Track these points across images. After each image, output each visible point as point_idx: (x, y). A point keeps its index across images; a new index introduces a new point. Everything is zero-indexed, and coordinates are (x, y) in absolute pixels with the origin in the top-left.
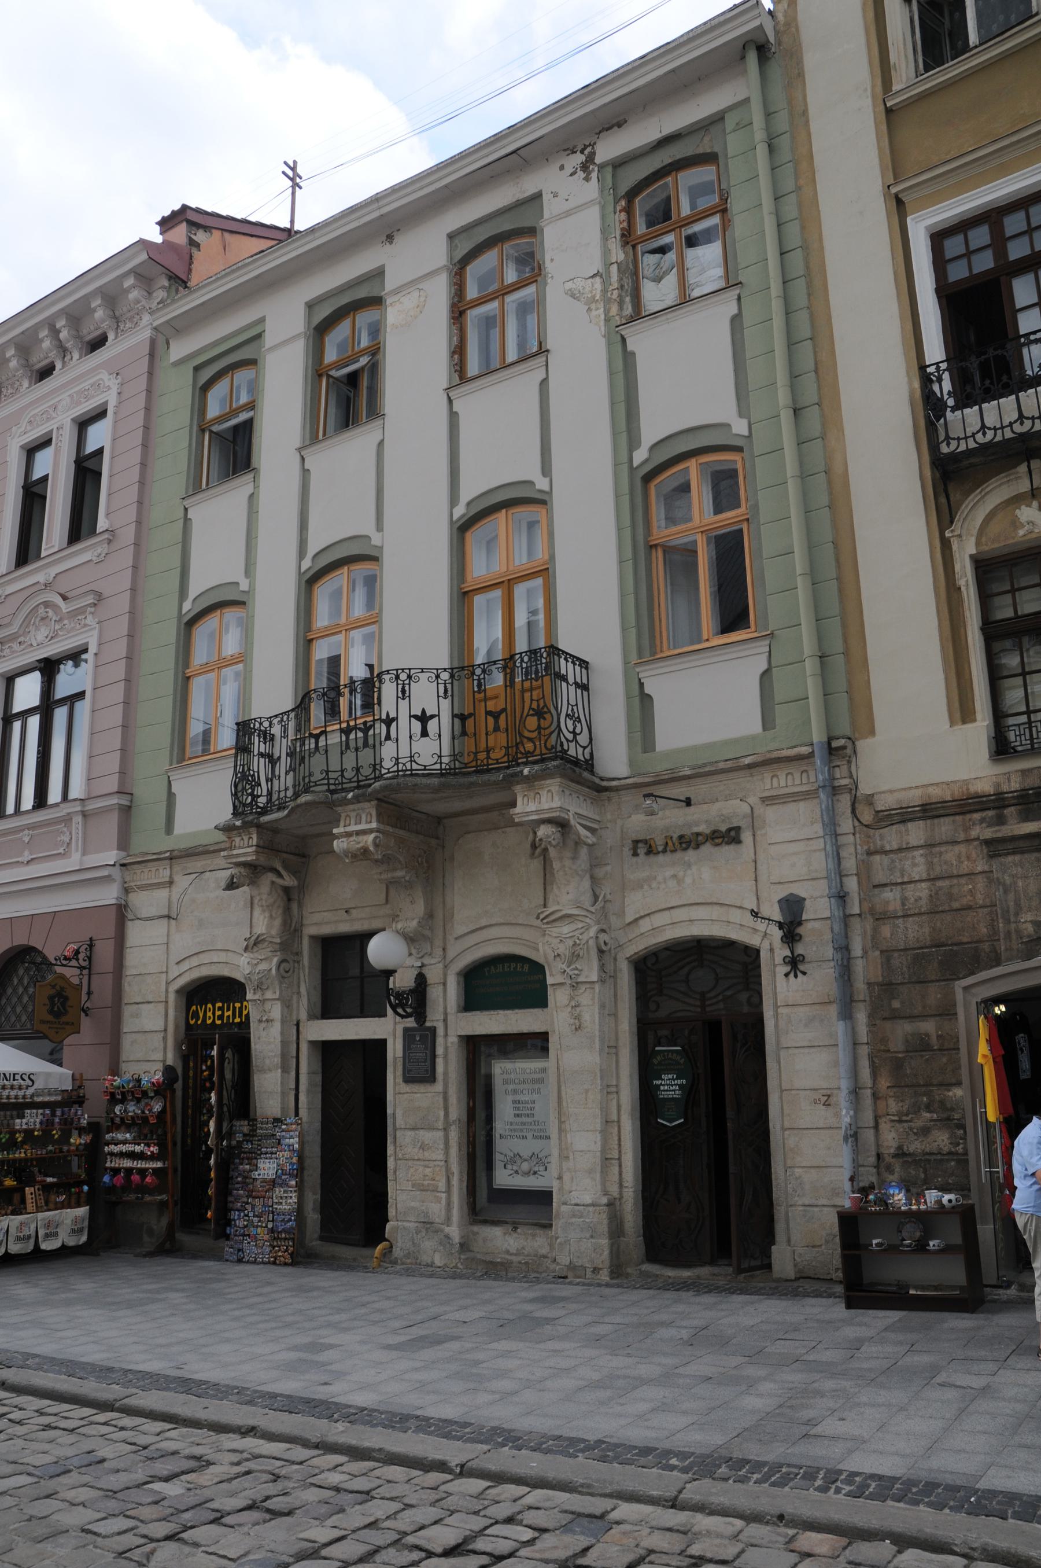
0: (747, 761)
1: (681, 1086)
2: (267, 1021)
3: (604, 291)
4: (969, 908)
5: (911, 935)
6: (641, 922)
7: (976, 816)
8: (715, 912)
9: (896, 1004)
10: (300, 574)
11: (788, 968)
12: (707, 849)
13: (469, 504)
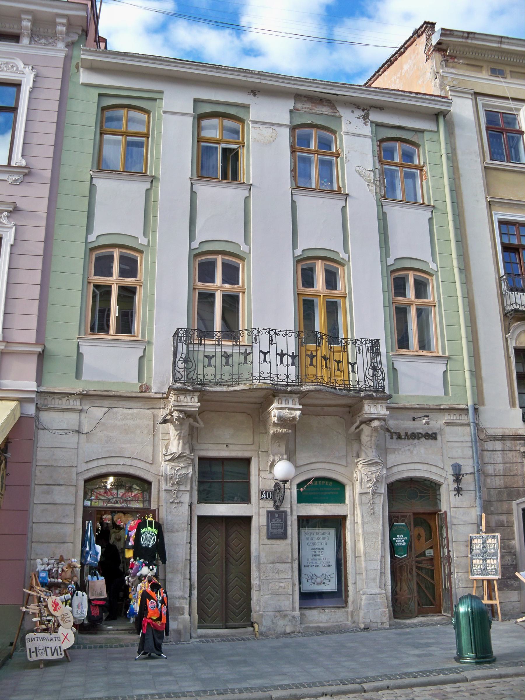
0: (442, 407)
1: (405, 541)
2: (179, 503)
3: (374, 180)
4: (516, 475)
5: (497, 483)
6: (393, 468)
7: (518, 442)
8: (425, 467)
9: (492, 509)
10: (190, 250)
11: (456, 492)
12: (423, 439)
13: (303, 251)
